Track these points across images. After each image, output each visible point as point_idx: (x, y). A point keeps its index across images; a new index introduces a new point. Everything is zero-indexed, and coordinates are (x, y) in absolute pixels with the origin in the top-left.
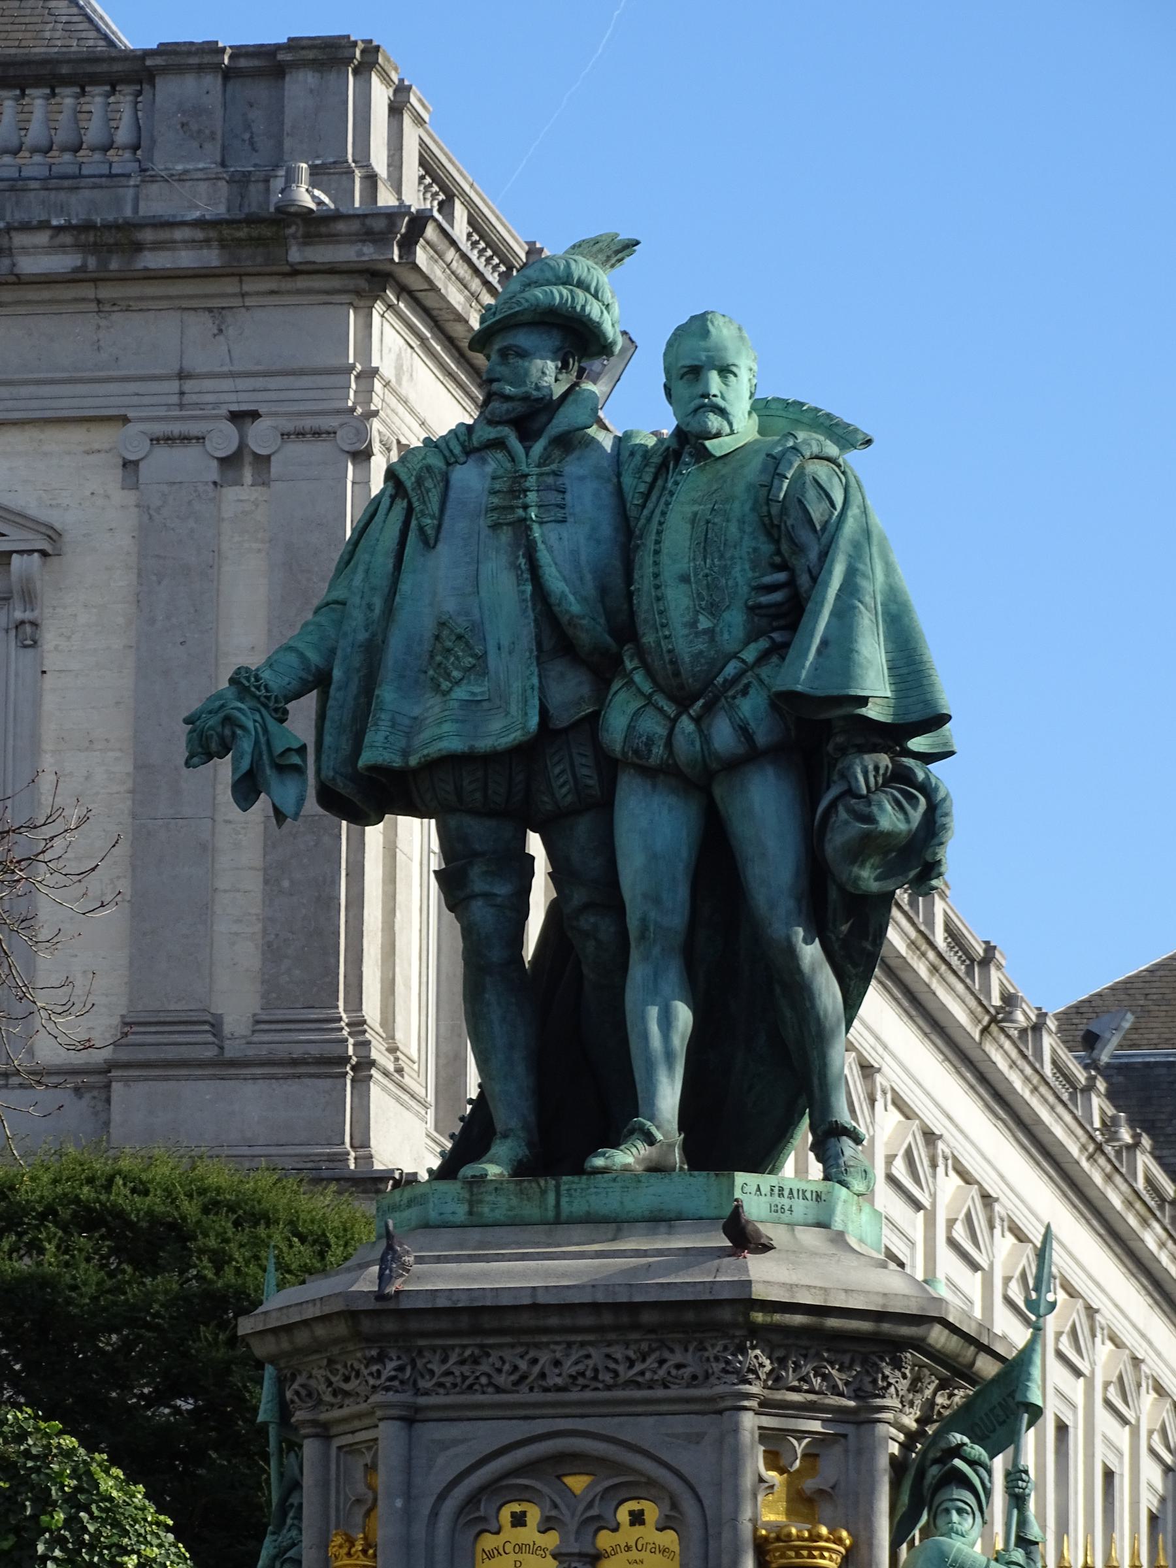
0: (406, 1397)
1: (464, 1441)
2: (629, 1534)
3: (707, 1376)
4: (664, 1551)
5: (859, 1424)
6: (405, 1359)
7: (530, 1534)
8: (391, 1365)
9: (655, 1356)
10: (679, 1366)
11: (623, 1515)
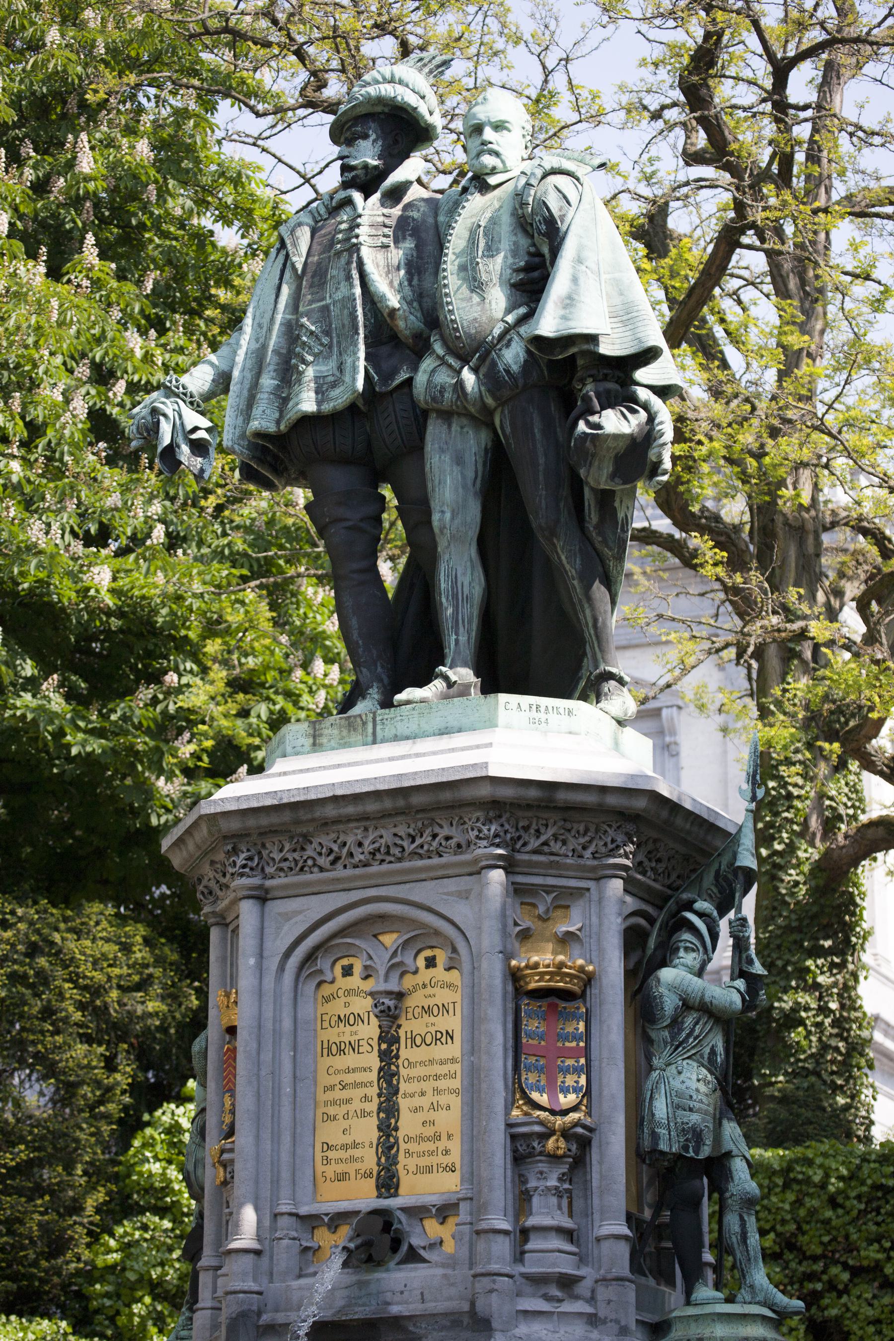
0: (256, 881)
1: (301, 912)
2: (425, 975)
3: (469, 843)
4: (450, 986)
5: (598, 879)
6: (253, 851)
7: (356, 981)
8: (242, 856)
9: (428, 832)
10: (447, 838)
11: (421, 962)
